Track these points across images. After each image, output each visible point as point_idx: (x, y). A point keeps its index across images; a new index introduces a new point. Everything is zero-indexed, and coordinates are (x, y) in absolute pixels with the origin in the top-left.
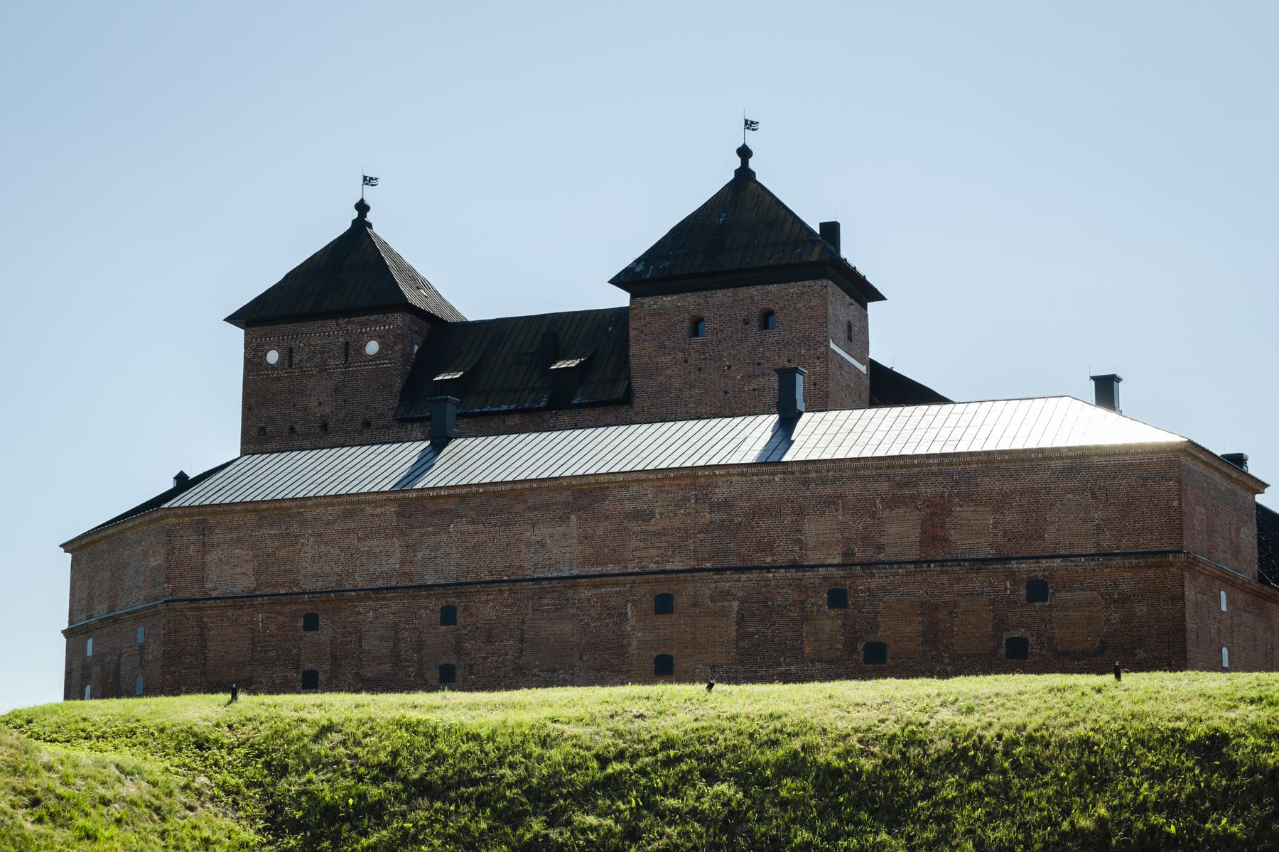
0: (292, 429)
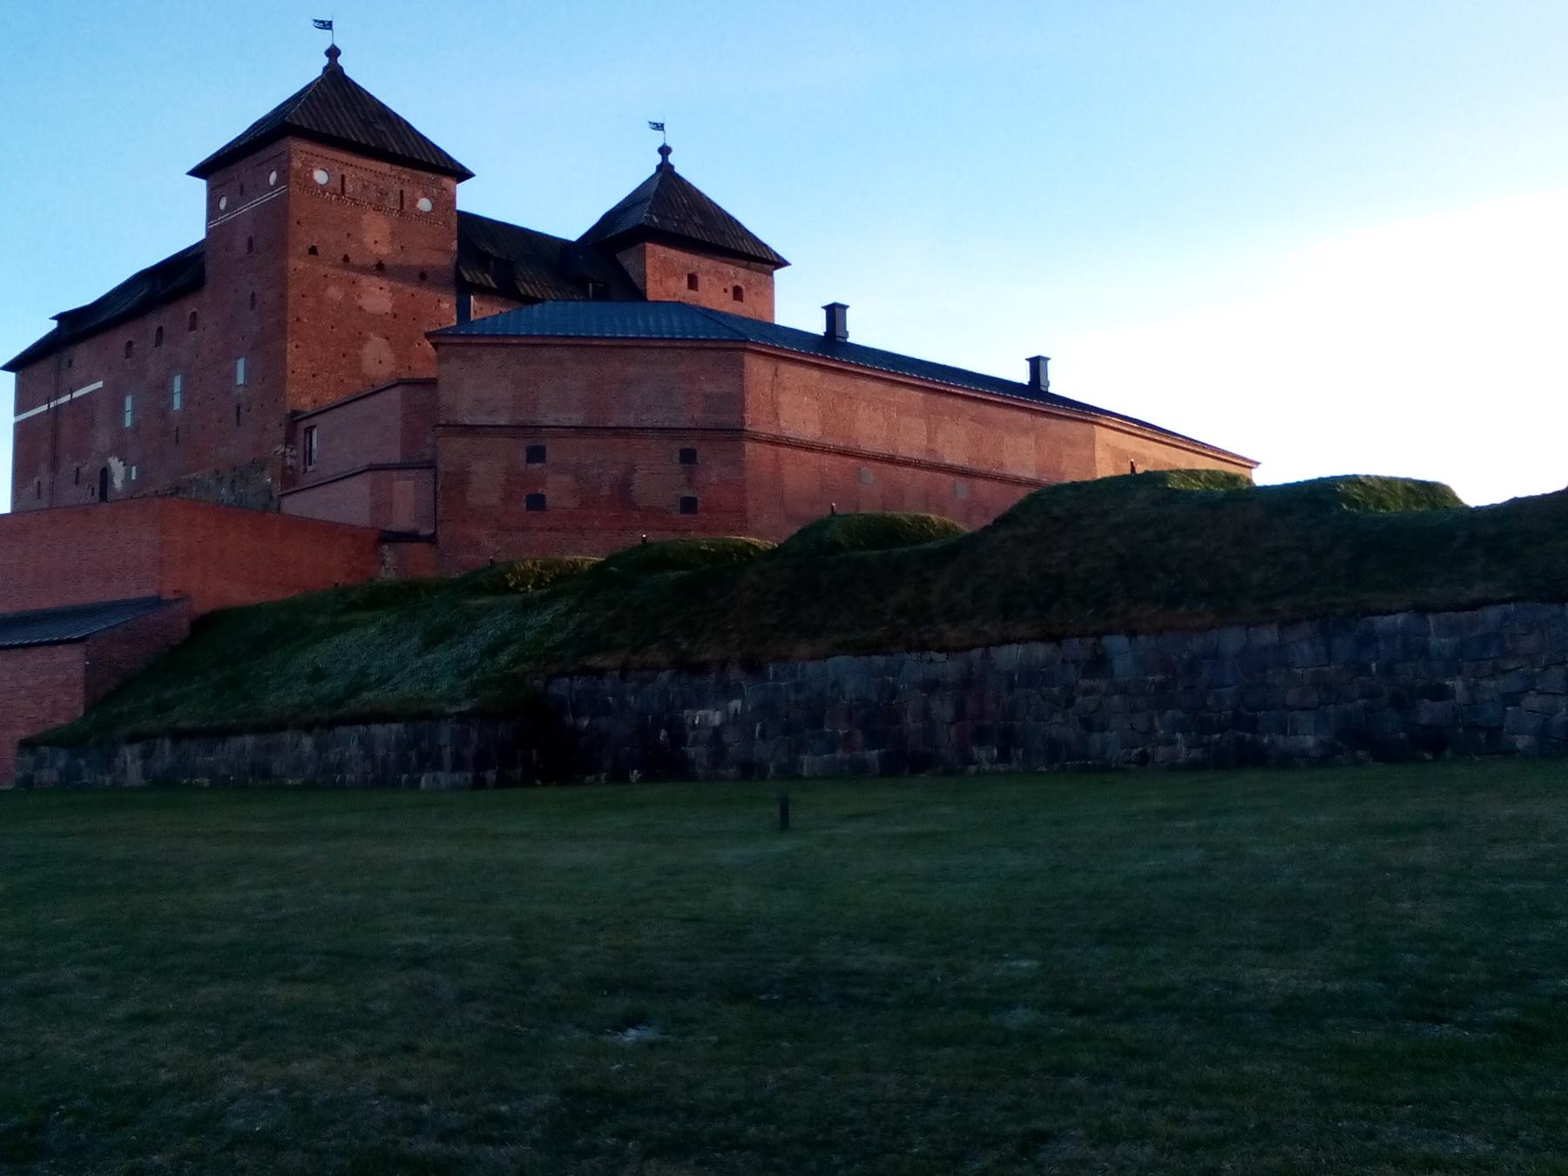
0: (346, 259)
